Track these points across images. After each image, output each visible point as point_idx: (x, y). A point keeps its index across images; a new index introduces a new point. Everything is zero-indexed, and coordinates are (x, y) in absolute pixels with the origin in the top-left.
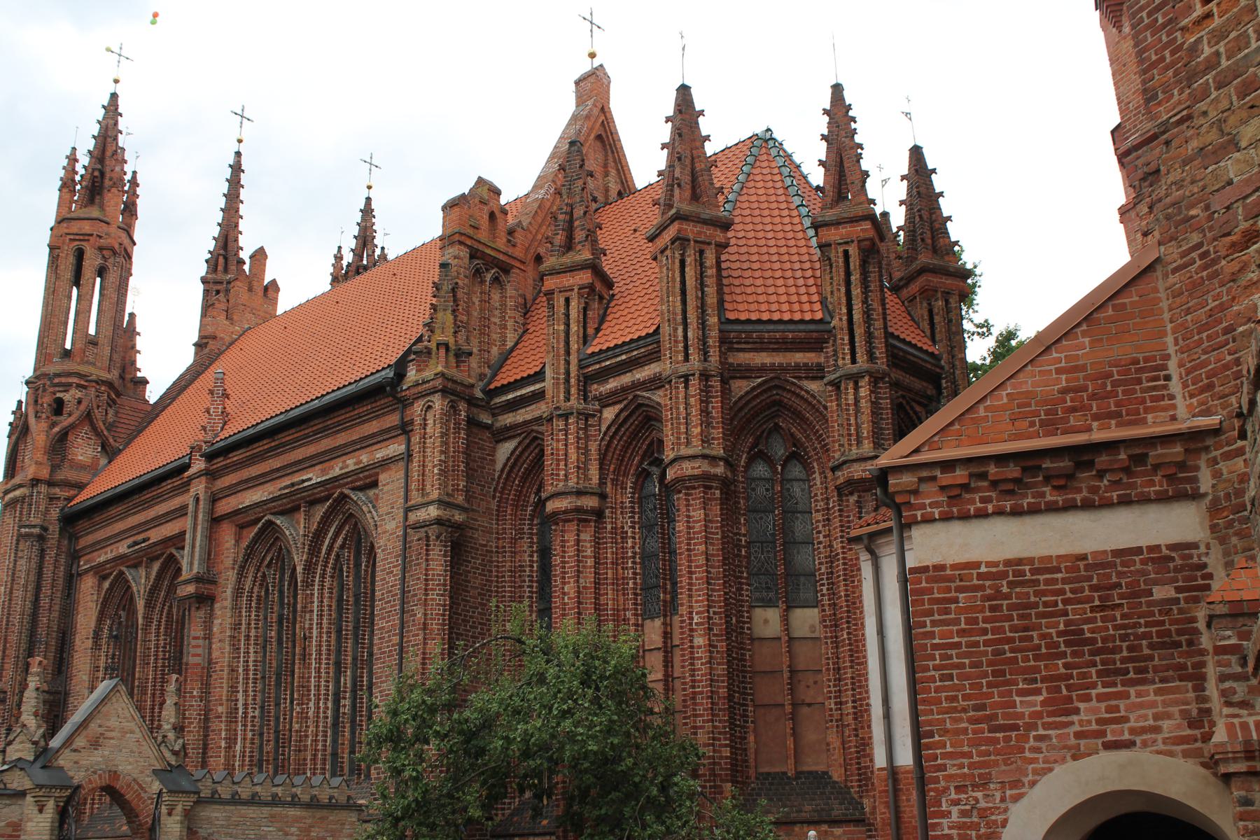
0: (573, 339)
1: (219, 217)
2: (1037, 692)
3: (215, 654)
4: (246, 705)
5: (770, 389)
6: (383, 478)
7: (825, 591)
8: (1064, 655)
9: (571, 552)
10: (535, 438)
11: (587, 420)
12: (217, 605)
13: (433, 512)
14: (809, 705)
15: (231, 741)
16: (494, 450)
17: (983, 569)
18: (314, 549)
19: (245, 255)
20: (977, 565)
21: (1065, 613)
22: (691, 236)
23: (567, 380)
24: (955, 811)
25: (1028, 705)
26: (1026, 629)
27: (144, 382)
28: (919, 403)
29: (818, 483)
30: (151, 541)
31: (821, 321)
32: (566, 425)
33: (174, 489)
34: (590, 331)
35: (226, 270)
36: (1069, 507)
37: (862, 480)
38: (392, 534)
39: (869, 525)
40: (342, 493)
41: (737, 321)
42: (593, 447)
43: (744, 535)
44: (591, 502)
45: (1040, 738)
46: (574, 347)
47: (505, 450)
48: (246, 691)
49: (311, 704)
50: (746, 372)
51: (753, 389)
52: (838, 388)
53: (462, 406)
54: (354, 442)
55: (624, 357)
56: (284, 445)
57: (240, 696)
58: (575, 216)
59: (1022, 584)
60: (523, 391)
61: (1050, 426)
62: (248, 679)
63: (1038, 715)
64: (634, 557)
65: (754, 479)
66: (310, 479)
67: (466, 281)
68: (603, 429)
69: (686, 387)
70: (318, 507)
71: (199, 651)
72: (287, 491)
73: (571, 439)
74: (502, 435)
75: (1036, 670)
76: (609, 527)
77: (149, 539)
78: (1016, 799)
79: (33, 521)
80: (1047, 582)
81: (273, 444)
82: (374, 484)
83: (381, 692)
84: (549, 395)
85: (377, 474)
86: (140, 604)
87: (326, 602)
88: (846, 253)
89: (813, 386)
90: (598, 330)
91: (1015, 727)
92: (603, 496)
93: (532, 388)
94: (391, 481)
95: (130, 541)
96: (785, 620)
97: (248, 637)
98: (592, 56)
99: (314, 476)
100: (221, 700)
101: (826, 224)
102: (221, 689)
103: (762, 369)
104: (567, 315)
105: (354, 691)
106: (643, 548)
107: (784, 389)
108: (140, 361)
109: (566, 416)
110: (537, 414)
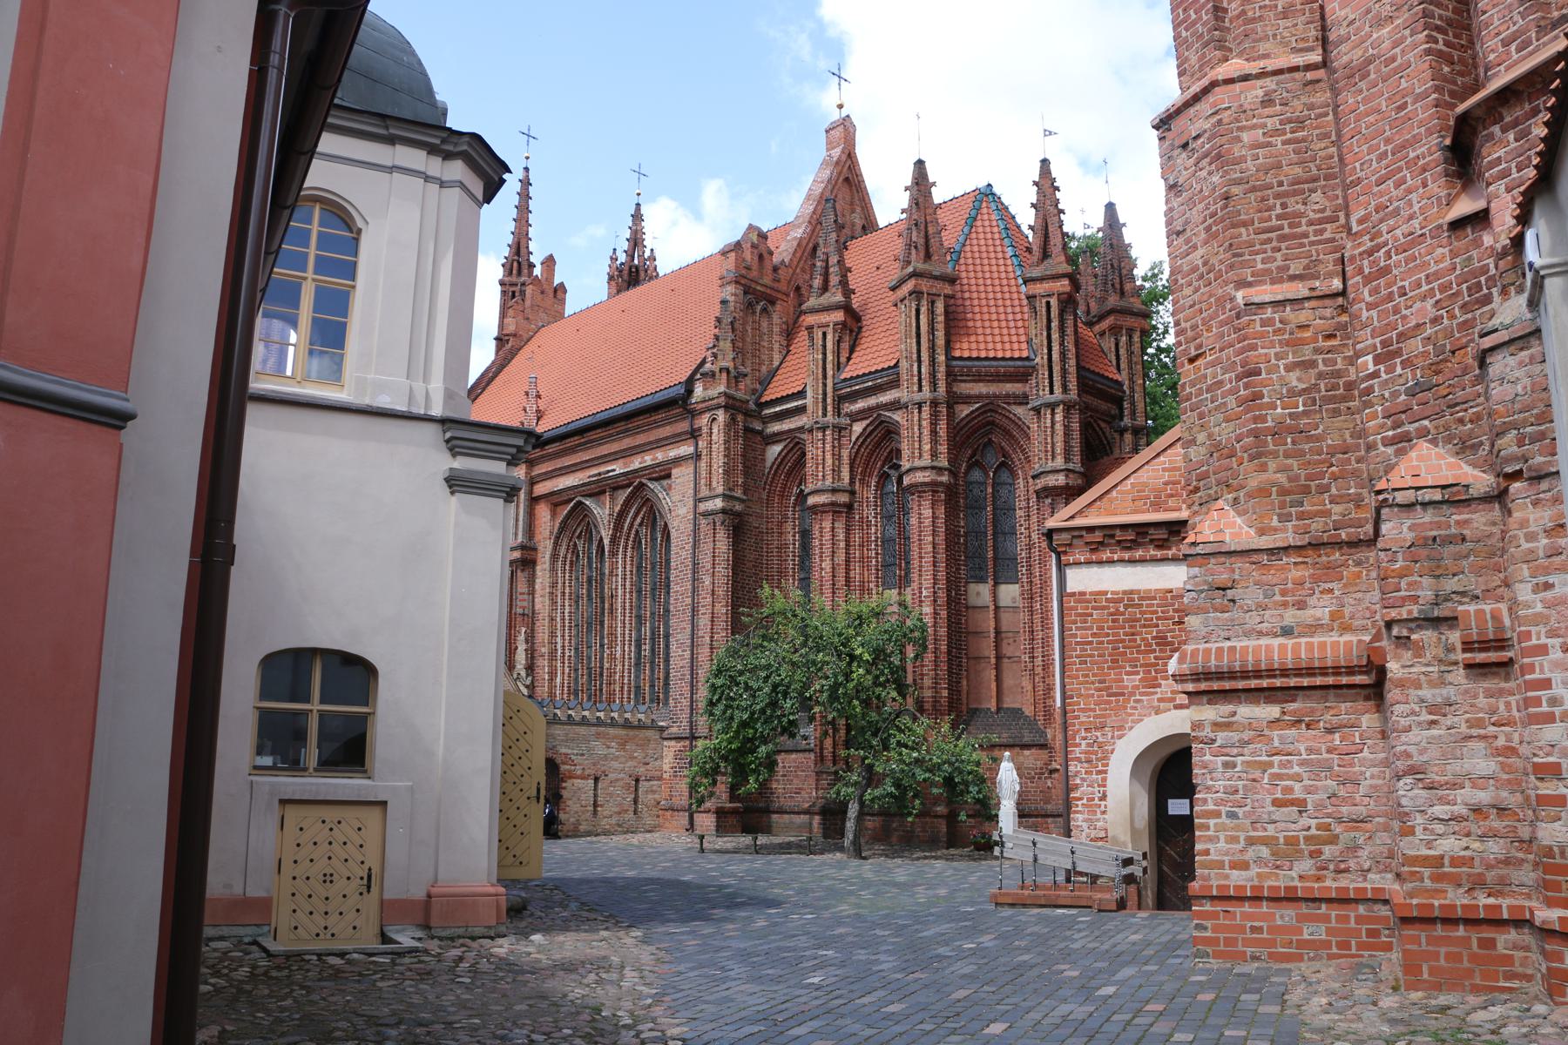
0: (829, 366)
1: (512, 226)
2: (1137, 673)
5: (985, 412)
6: (674, 472)
8: (1155, 651)
9: (827, 536)
10: (798, 443)
13: (718, 503)
15: (552, 675)
16: (764, 451)
17: (1109, 596)
18: (618, 526)
19: (537, 259)
20: (1106, 593)
21: (1157, 626)
22: (925, 290)
23: (824, 400)
24: (1084, 743)
25: (1130, 681)
26: (1133, 634)
28: (1104, 421)
31: (1027, 359)
34: (843, 360)
35: (519, 273)
36: (1164, 560)
37: (1055, 488)
41: (961, 358)
42: (845, 453)
44: (843, 498)
45: (1137, 701)
46: (830, 373)
47: (775, 450)
49: (618, 648)
50: (967, 399)
51: (972, 412)
52: (1039, 413)
53: (740, 418)
54: (650, 443)
57: (559, 640)
59: (1132, 606)
60: (788, 406)
61: (1157, 506)
63: (1137, 687)
65: (971, 483)
68: (853, 439)
69: (920, 412)
70: (620, 491)
73: (828, 447)
75: (1137, 660)
78: (1120, 737)
80: (1148, 606)
82: (668, 476)
84: (810, 409)
87: (628, 569)
88: (1048, 303)
89: (1019, 411)
90: (849, 359)
91: (1123, 694)
92: (852, 493)
93: (796, 404)
94: (683, 475)
97: (563, 593)
98: (840, 107)
99: (618, 468)
101: (1033, 280)
102: (542, 634)
103: (979, 397)
104: (824, 346)
105: (653, 639)
106: (883, 533)
109: (823, 429)
110: (800, 424)
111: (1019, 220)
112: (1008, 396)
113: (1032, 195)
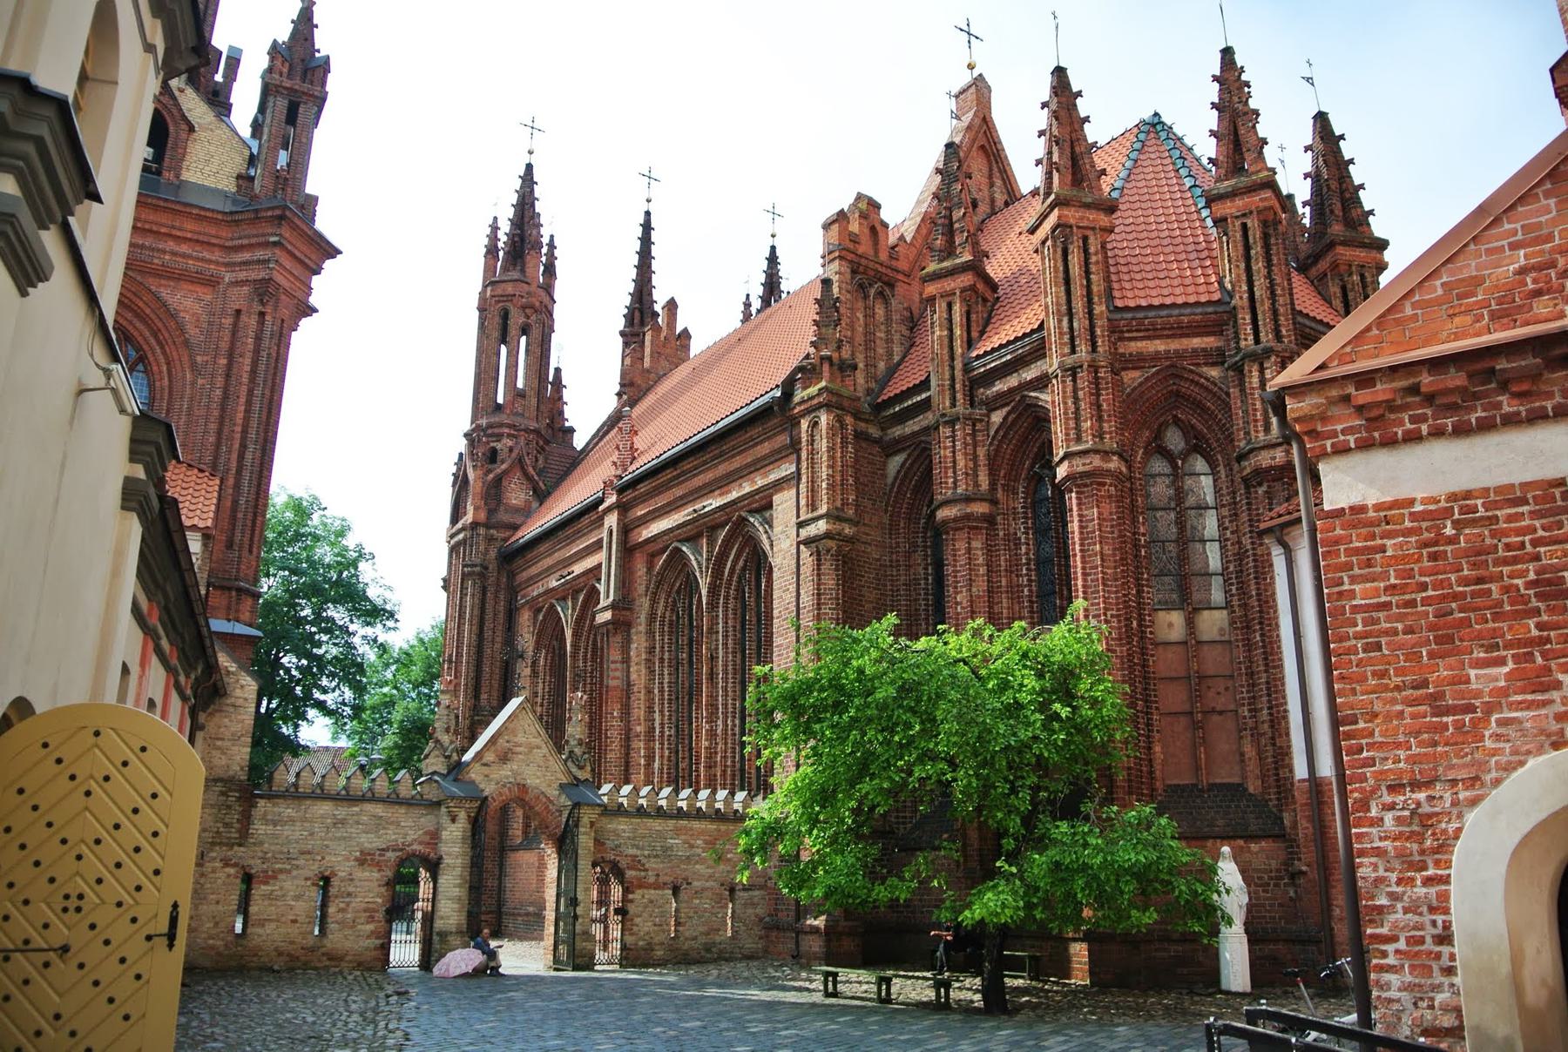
0: (958, 343)
1: (633, 273)
2: (1502, 662)
3: (633, 676)
4: (662, 724)
6: (777, 499)
7: (1234, 591)
8: (1537, 612)
9: (962, 561)
10: (925, 449)
11: (974, 425)
12: (633, 630)
13: (822, 526)
14: (1221, 713)
15: (650, 758)
16: (885, 464)
17: (1418, 508)
18: (717, 573)
19: (658, 308)
20: (1412, 502)
21: (1537, 558)
22: (1072, 221)
23: (953, 386)
24: (1389, 818)
25: (1485, 679)
26: (1480, 580)
27: (571, 430)
29: (1223, 476)
31: (1219, 302)
32: (953, 431)
33: (593, 522)
34: (975, 334)
36: (1536, 418)
39: (1280, 516)
41: (1127, 309)
42: (981, 452)
43: (1144, 535)
44: (980, 508)
45: (1502, 723)
46: (959, 351)
47: (896, 462)
48: (661, 711)
49: (720, 722)
50: (1138, 362)
51: (1147, 379)
52: (1242, 372)
53: (849, 420)
54: (748, 466)
55: (1009, 357)
56: (683, 473)
58: (954, 219)
59: (1474, 523)
61: (1503, 316)
62: (663, 699)
63: (1504, 692)
64: (1028, 564)
65: (1153, 476)
67: (849, 296)
68: (992, 433)
69: (1074, 381)
71: (618, 674)
74: (891, 448)
75: (1495, 633)
76: (1001, 533)
78: (1474, 802)
80: (1510, 518)
82: (769, 506)
84: (935, 401)
85: (771, 496)
86: (568, 633)
88: (1244, 226)
90: (982, 333)
91: (1470, 709)
94: (784, 504)
95: (557, 575)
96: (1190, 623)
98: (971, 67)
99: (714, 502)
101: (1221, 197)
102: (639, 711)
103: (1156, 357)
106: (1037, 553)
107: (1181, 378)
108: (568, 412)
109: (952, 423)
110: (925, 423)
111: (1197, 152)
112: (1195, 352)
113: (1212, 119)
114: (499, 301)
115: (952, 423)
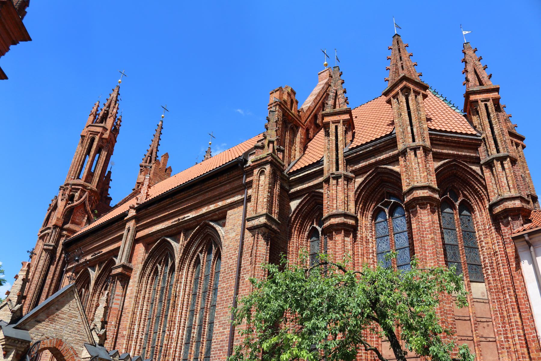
7: (489, 273)
27: (110, 199)
29: (478, 216)
30: (103, 253)
33: (119, 227)
38: (233, 239)
39: (519, 232)
40: (205, 223)
49: (175, 331)
54: (216, 196)
55: (371, 148)
56: (177, 201)
57: (136, 327)
58: (338, 94)
64: (373, 253)
66: (189, 216)
71: (119, 302)
72: (175, 223)
77: (102, 252)
79: (51, 243)
81: (171, 201)
82: (224, 217)
83: (219, 322)
87: (189, 279)
88: (486, 105)
92: (356, 220)
93: (315, 170)
100: (126, 328)
102: (126, 322)
103: (448, 156)
105: (200, 326)
108: (110, 191)
109: (337, 178)
114: (90, 134)
115: (337, 178)
